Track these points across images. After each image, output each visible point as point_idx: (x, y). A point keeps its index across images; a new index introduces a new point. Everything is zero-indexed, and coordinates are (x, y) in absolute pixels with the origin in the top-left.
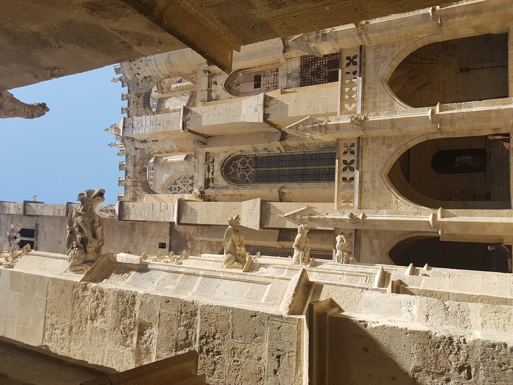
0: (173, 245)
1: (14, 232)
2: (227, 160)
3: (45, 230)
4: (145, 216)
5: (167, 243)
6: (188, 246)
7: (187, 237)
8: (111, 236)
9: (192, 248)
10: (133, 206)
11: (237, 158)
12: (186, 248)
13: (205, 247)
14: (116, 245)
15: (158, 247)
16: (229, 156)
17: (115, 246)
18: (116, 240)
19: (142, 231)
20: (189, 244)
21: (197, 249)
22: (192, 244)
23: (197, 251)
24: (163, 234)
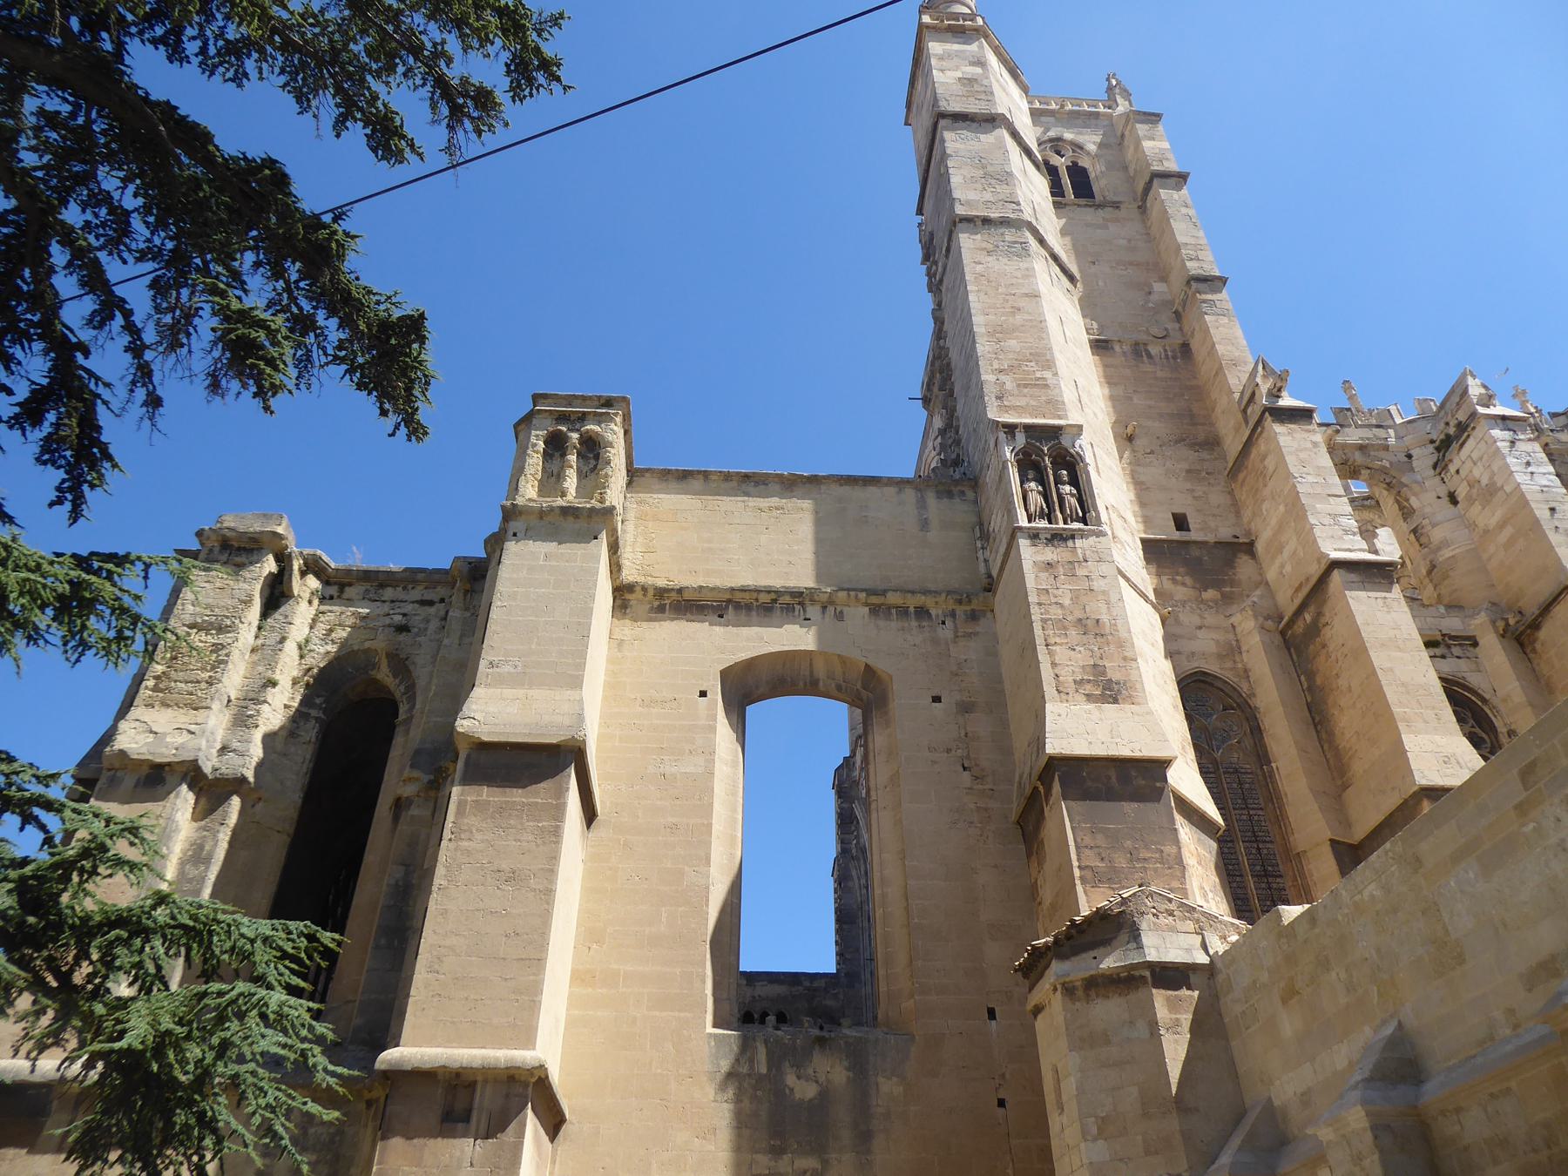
0: (1195, 552)
1: (1074, 151)
2: (1469, 695)
3: (1109, 224)
5: (1194, 535)
7: (1228, 589)
10: (1315, 444)
16: (1484, 700)
17: (1135, 401)
18: (1152, 403)
19: (1199, 468)
20: (1210, 594)
23: (1202, 617)
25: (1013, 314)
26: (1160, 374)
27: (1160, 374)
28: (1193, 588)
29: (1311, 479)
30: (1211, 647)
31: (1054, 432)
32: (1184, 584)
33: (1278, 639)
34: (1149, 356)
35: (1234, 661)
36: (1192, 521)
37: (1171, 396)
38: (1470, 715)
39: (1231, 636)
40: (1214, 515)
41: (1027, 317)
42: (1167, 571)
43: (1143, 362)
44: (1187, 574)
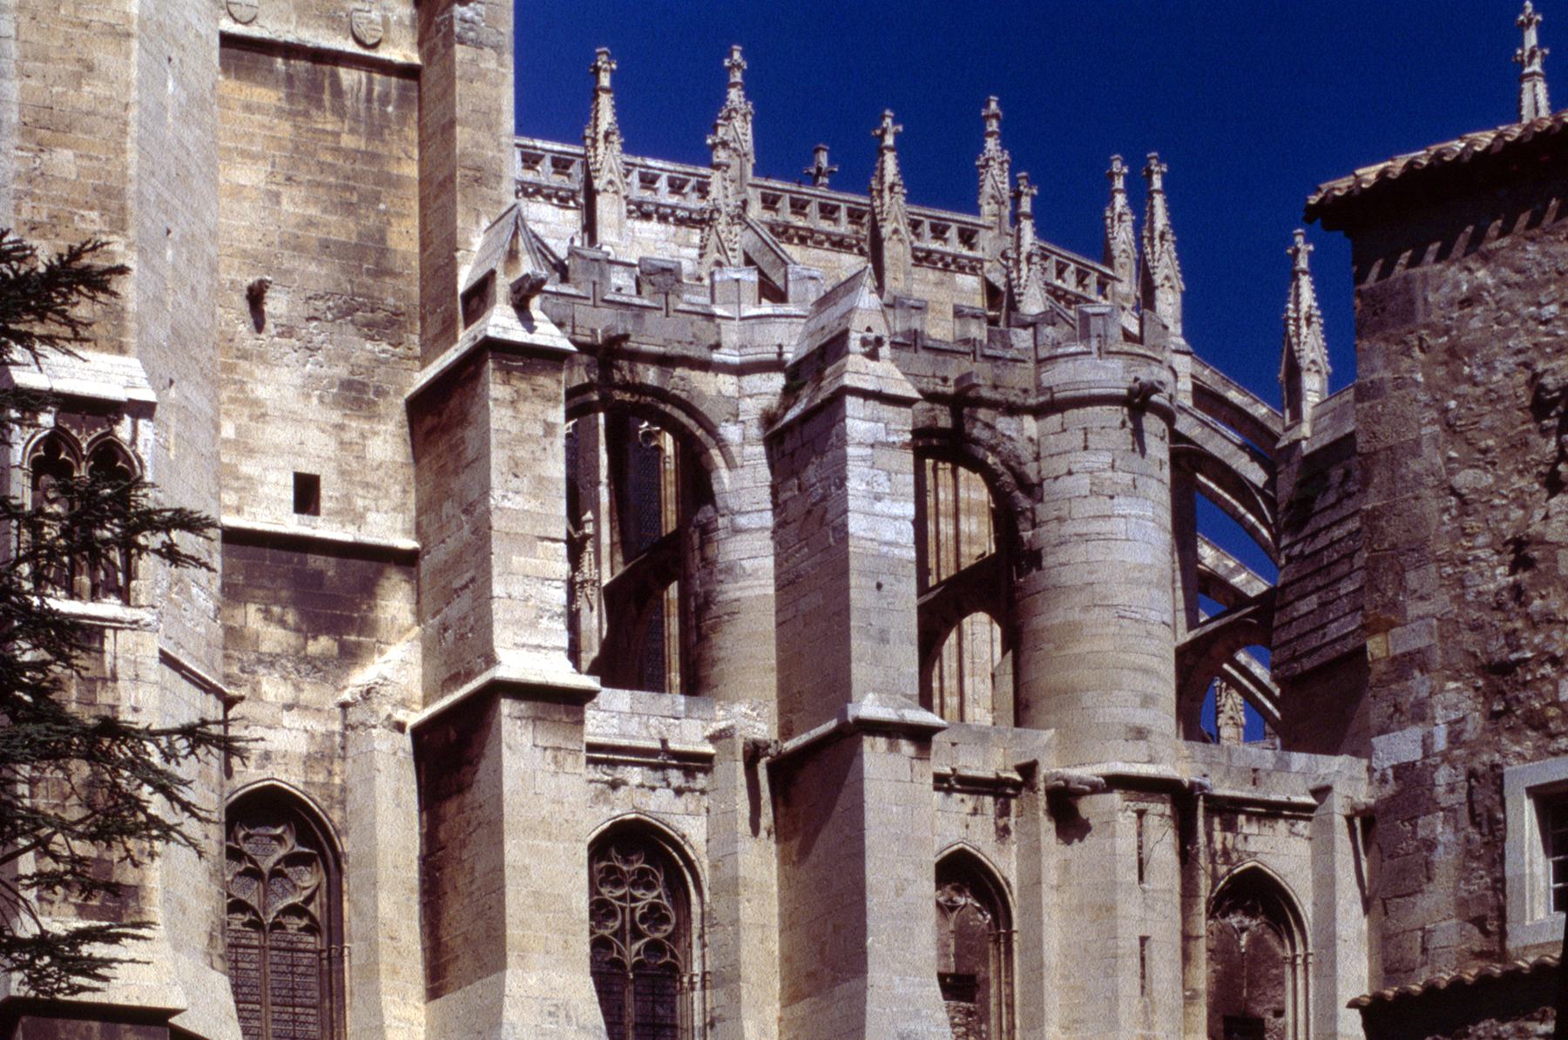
4: (510, 495)
6: (315, 638)
7: (353, 638)
8: (332, 179)
9: (308, 660)
11: (681, 900)
12: (304, 627)
13: (319, 727)
14: (291, 209)
15: (299, 470)
17: (286, 205)
18: (313, 211)
20: (322, 645)
21: (307, 687)
22: (325, 659)
24: (360, 503)
25: (77, 80)
26: (348, 141)
27: (348, 141)
28: (297, 630)
29: (517, 503)
30: (301, 745)
31: (106, 410)
32: (282, 623)
33: (406, 741)
34: (338, 92)
35: (330, 773)
36: (328, 493)
37: (355, 199)
38: (661, 879)
39: (337, 727)
40: (367, 485)
41: (101, 89)
42: (261, 593)
43: (319, 105)
44: (298, 603)
